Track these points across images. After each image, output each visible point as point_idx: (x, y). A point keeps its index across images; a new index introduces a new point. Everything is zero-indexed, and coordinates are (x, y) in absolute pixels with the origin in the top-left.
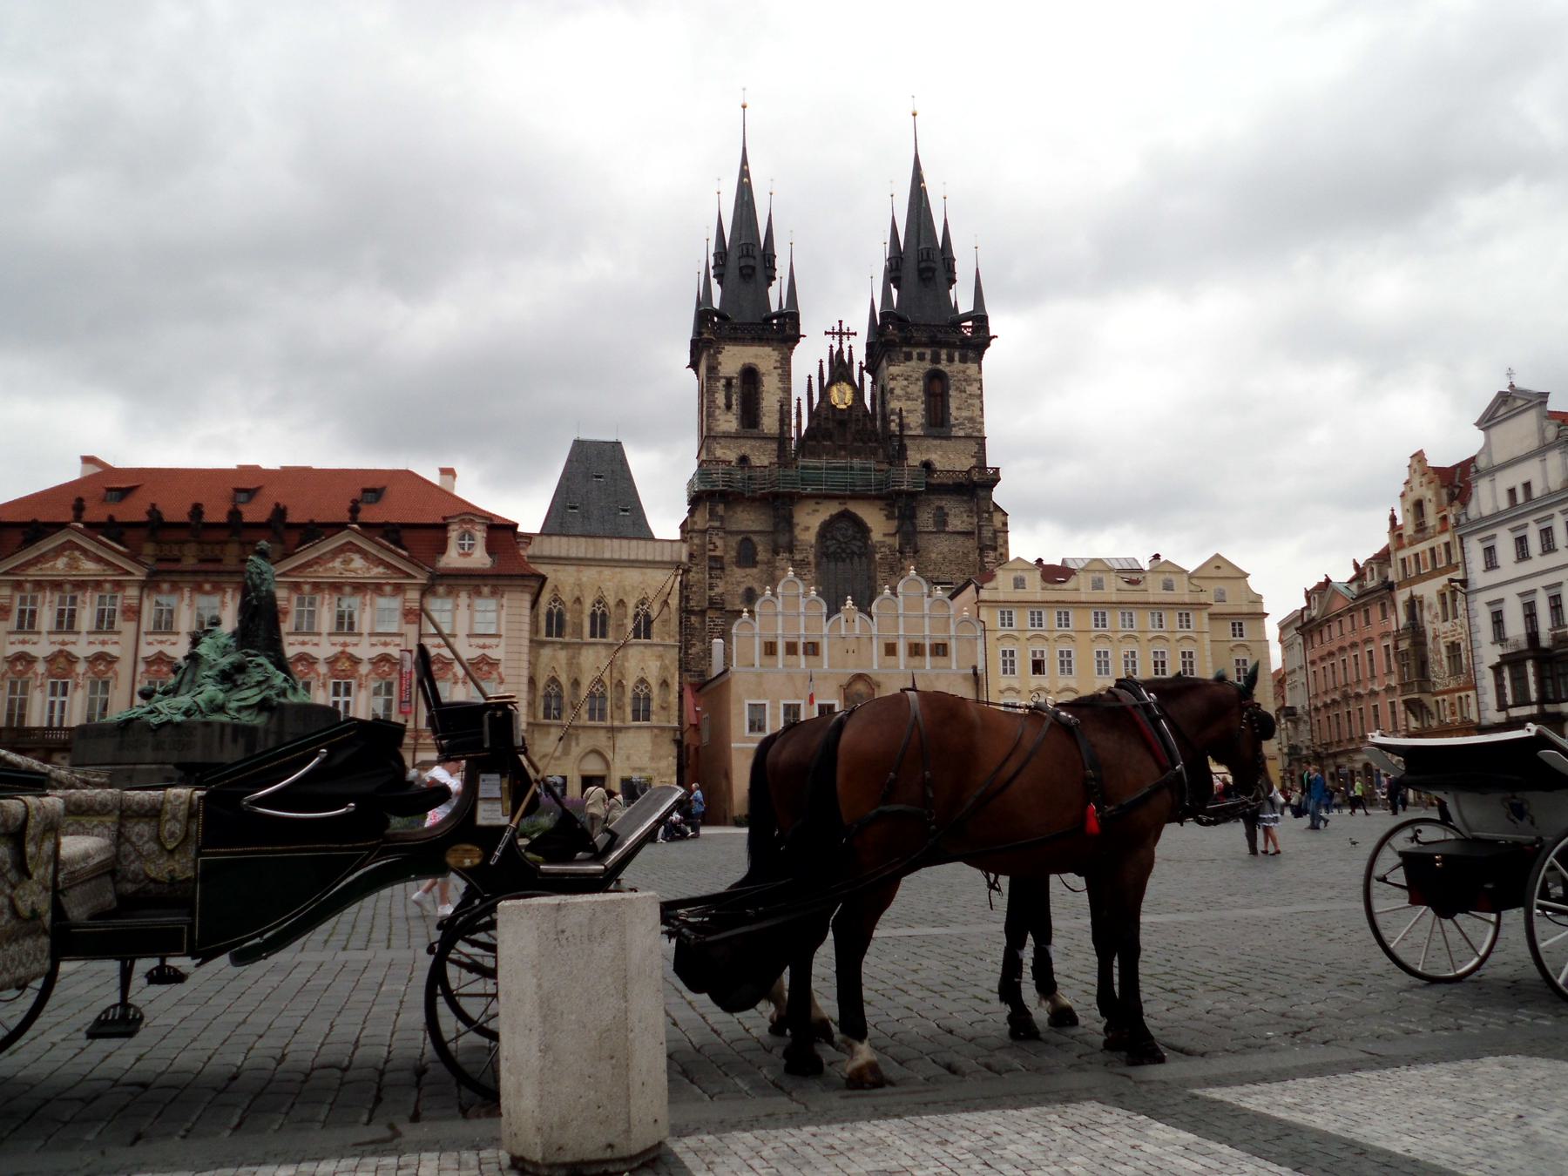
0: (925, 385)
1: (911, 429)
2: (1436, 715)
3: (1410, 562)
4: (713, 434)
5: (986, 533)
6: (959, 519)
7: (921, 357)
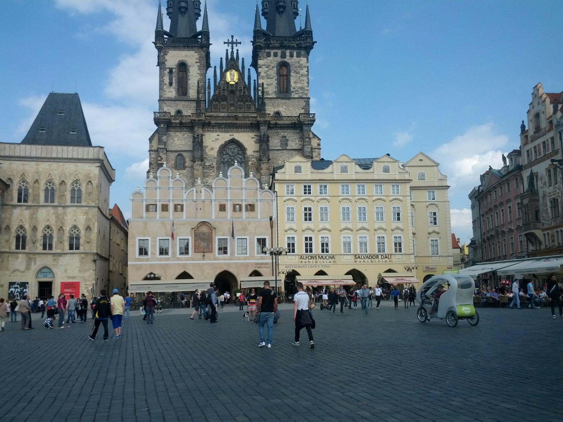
0: (277, 70)
2: (543, 243)
3: (531, 152)
4: (162, 99)
5: (307, 149)
6: (294, 142)
7: (276, 55)
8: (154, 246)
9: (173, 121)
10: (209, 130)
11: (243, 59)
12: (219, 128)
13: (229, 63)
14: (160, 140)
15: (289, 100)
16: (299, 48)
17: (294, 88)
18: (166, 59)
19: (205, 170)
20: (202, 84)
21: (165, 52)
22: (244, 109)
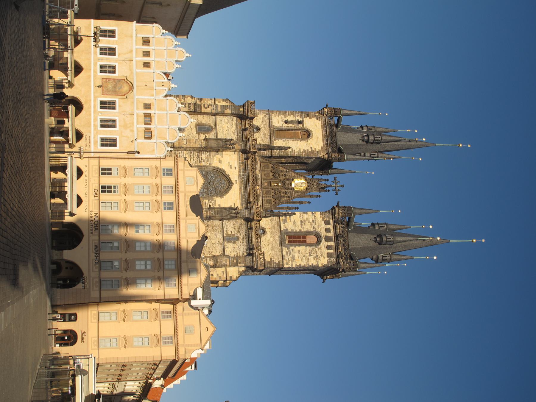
4: (270, 113)
7: (327, 230)
8: (109, 42)
9: (247, 122)
10: (241, 159)
11: (320, 196)
12: (243, 169)
13: (315, 182)
15: (279, 244)
16: (338, 256)
17: (293, 250)
18: (312, 118)
19: (196, 154)
21: (319, 117)
22: (266, 197)
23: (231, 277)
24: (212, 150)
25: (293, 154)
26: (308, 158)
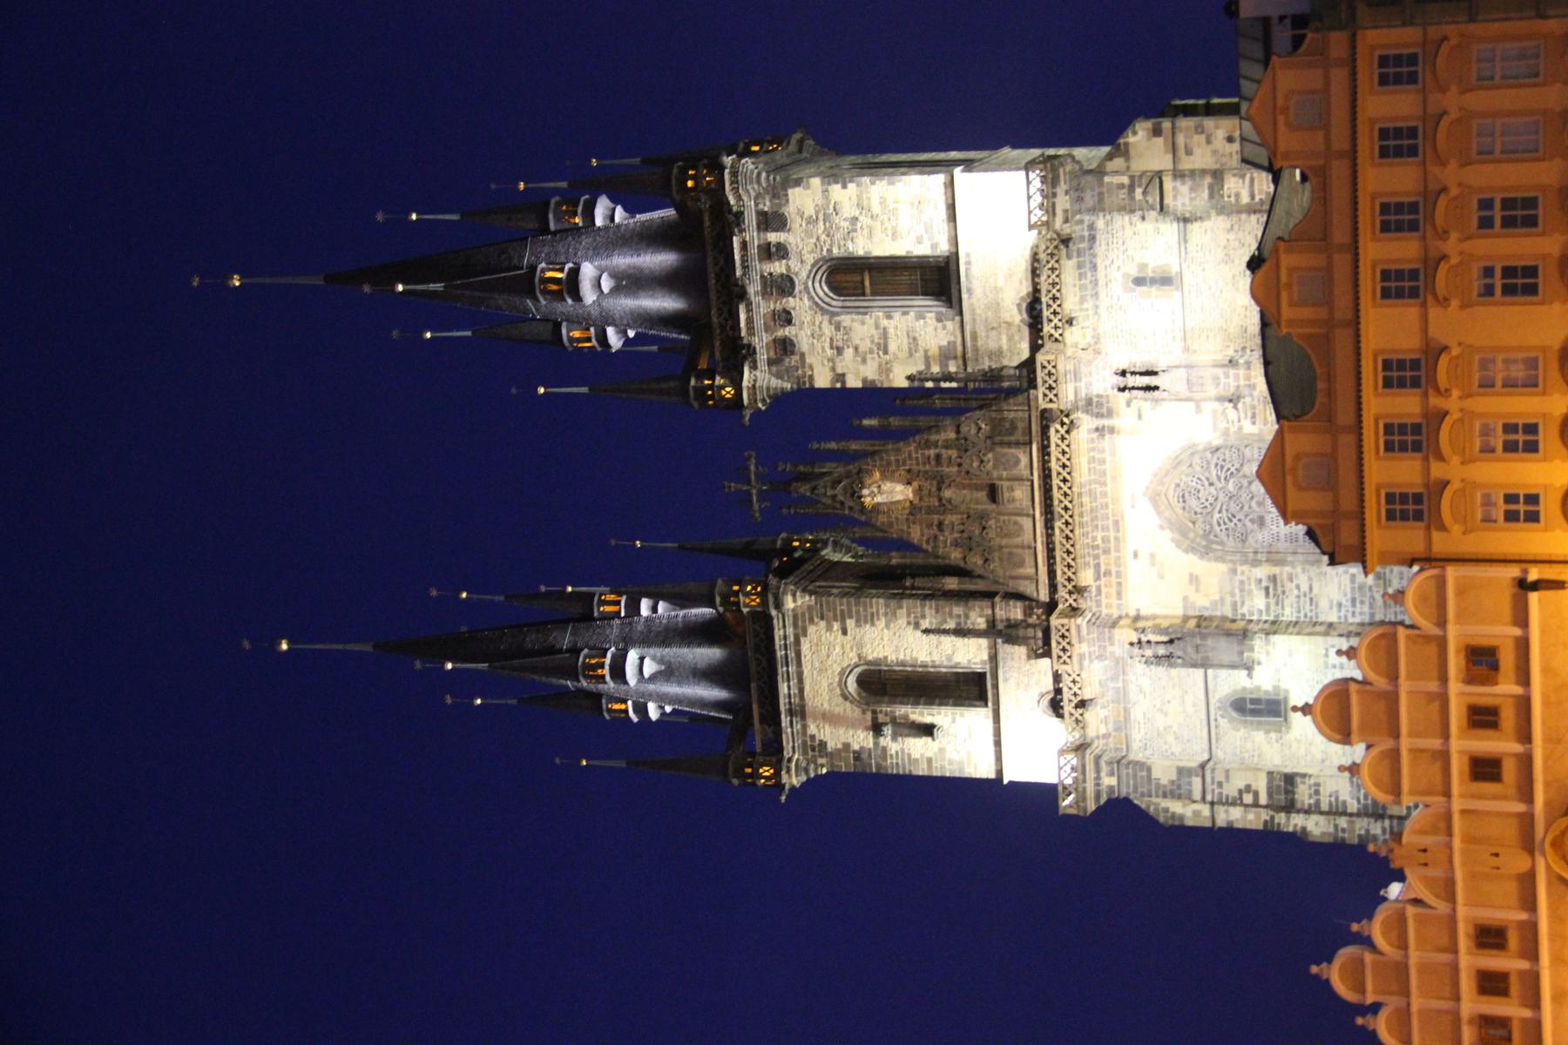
1: (951, 344)
7: (786, 318)
10: (1114, 591)
12: (1107, 552)
14: (1172, 792)
17: (919, 241)
18: (839, 746)
19: (1288, 611)
20: (927, 611)
21: (813, 749)
23: (1157, 132)
24: (1228, 625)
25: (915, 607)
26: (857, 593)
